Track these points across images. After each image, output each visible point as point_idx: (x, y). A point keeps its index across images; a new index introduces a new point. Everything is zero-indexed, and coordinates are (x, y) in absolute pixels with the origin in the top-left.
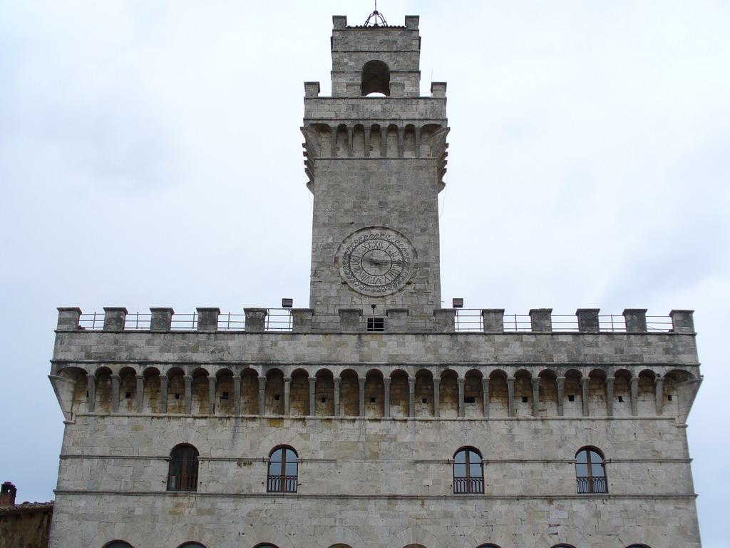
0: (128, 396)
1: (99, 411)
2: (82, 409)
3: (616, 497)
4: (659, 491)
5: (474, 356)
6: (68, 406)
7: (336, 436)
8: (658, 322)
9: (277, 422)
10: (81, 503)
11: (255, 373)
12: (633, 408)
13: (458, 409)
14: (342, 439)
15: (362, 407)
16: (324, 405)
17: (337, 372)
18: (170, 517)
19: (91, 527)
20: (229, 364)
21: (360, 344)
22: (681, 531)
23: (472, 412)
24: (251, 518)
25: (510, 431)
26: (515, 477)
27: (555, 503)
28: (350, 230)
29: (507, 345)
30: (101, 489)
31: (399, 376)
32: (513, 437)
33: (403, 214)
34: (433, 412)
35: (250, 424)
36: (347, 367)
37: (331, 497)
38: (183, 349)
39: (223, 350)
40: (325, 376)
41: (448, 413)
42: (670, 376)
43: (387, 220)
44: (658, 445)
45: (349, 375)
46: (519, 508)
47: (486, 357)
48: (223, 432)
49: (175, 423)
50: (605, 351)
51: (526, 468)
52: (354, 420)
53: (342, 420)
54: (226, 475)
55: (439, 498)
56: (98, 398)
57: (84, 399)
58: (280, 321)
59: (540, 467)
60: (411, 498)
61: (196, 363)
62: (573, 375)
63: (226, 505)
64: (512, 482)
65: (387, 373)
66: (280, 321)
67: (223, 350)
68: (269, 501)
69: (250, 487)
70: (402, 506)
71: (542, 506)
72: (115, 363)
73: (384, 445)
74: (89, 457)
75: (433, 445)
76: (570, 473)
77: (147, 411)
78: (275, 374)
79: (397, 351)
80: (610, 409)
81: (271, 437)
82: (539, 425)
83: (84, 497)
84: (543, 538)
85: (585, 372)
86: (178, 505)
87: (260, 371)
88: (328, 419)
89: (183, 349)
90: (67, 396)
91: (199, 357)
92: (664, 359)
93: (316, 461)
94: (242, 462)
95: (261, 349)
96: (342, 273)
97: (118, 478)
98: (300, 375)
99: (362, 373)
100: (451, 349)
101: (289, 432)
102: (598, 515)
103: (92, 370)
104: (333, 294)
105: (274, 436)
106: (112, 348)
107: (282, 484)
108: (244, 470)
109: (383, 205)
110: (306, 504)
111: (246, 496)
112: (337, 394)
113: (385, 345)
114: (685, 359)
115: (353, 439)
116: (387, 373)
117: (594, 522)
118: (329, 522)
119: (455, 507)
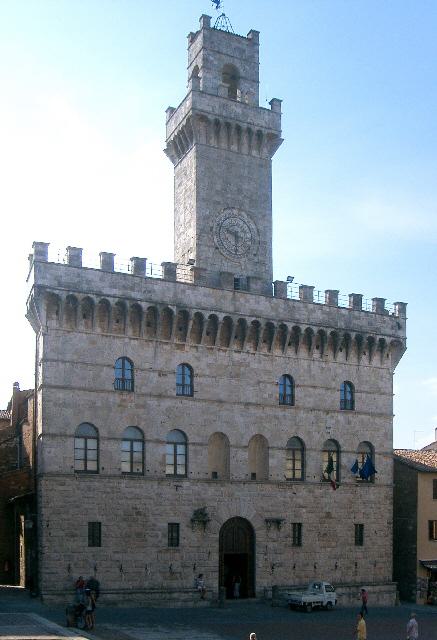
0: (84, 317)
1: (66, 326)
2: (54, 324)
3: (359, 413)
4: (378, 411)
5: (297, 316)
6: (44, 320)
7: (216, 360)
8: (390, 307)
9: (181, 347)
10: (61, 395)
11: (170, 312)
12: (370, 360)
13: (283, 349)
14: (219, 363)
15: (232, 342)
16: (208, 338)
17: (221, 316)
18: (119, 409)
19: (68, 412)
20: (156, 303)
21: (234, 299)
22: (386, 434)
23: (290, 352)
24: (169, 410)
25: (309, 366)
26: (310, 396)
27: (329, 415)
28: (219, 207)
29: (313, 311)
30: (73, 385)
31: (256, 324)
32: (310, 371)
33: (251, 201)
34: (270, 349)
35: (165, 347)
36: (227, 315)
37: (213, 402)
38: (124, 287)
39: (150, 292)
40: (213, 318)
41: (277, 352)
42: (392, 343)
43: (242, 204)
44: (381, 384)
45: (228, 320)
46: (312, 416)
47: (305, 319)
48: (149, 351)
49: (117, 341)
50: (363, 323)
51: (317, 391)
52: (225, 351)
53: (219, 350)
54: (151, 382)
55: (272, 406)
56: (64, 317)
57: (54, 316)
58: (184, 275)
59: (323, 391)
60: (257, 405)
61: (134, 299)
62: (347, 337)
63: (152, 402)
64: (309, 399)
65: (249, 321)
66: (184, 275)
67: (150, 292)
68: (178, 401)
69: (166, 391)
70: (252, 410)
71: (322, 415)
72: (80, 292)
73: (242, 369)
74: (64, 362)
75: (268, 372)
76: (337, 396)
77: (99, 330)
78: (185, 314)
79: (253, 306)
80: (359, 359)
81: (178, 357)
82: (324, 365)
83: (62, 390)
84: (322, 435)
85: (353, 335)
86: (124, 400)
87: (174, 309)
88: (212, 349)
89: (124, 287)
90: (44, 313)
91: (134, 294)
92: (389, 331)
93: (204, 376)
94: (161, 374)
95: (175, 295)
96: (215, 240)
97: (84, 379)
98: (199, 316)
99: (235, 319)
100: (285, 310)
101: (188, 355)
102: (349, 423)
103: (64, 295)
104: (211, 256)
105: (180, 357)
106: (77, 280)
107: (187, 390)
108: (163, 379)
109: (240, 191)
110: (198, 404)
111: (164, 397)
112: (219, 331)
113: (247, 301)
114: (400, 333)
115: (225, 363)
116: (249, 321)
117: (347, 426)
118: (213, 417)
119: (279, 412)
